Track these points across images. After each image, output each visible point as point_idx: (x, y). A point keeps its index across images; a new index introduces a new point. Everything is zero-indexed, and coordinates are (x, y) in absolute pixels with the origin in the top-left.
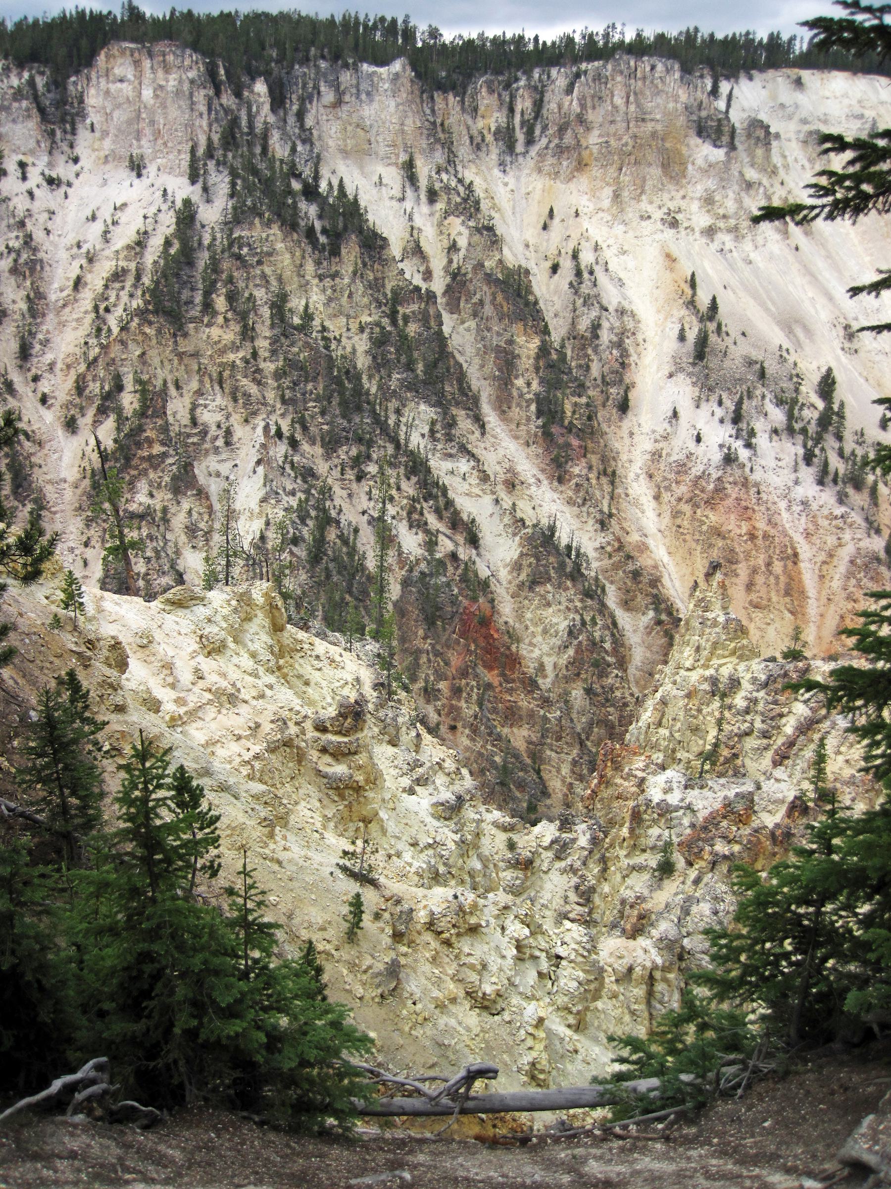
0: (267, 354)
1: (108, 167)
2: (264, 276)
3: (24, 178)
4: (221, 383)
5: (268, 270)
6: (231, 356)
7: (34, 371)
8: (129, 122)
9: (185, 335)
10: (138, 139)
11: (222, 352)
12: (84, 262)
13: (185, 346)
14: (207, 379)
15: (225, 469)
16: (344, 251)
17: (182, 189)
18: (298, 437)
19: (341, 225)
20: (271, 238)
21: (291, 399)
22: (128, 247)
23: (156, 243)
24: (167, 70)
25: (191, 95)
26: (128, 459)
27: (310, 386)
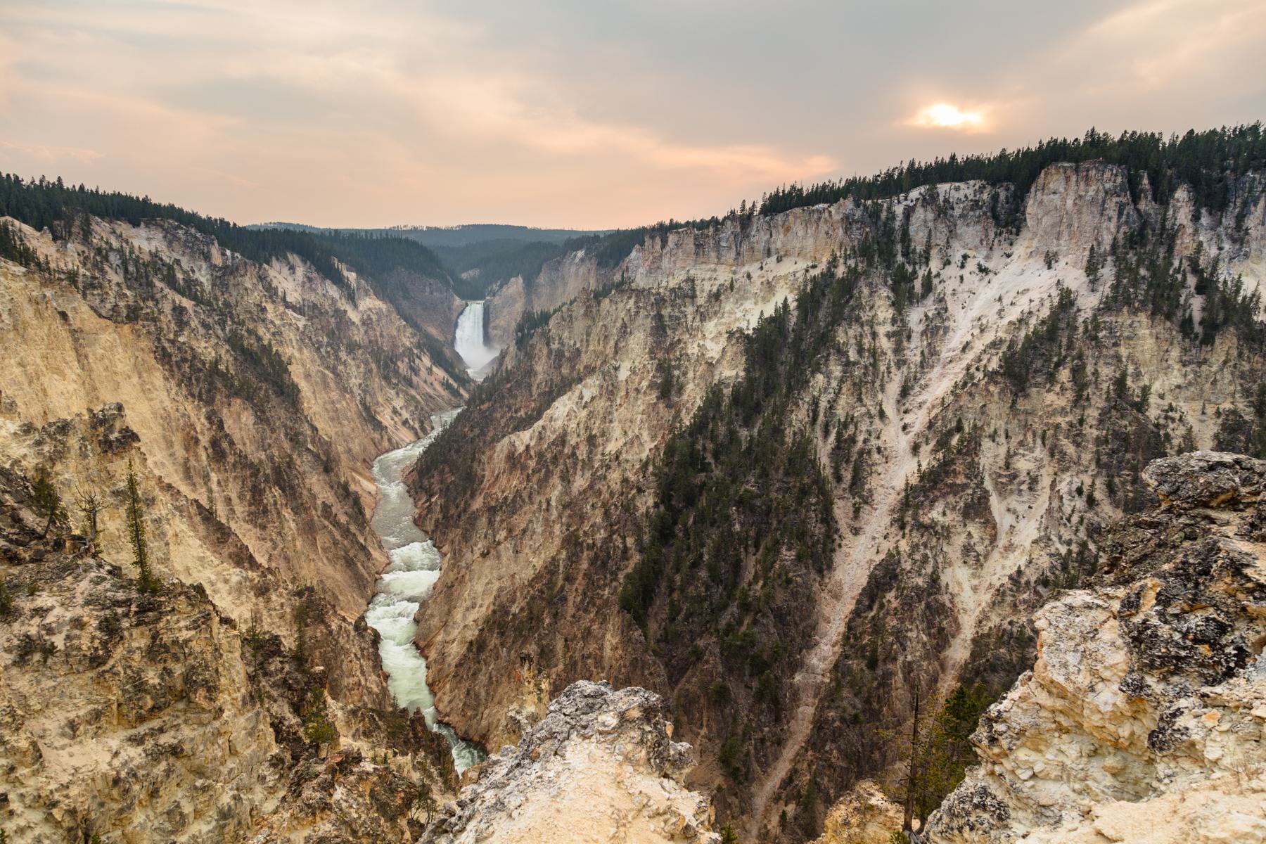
0: (1094, 422)
1: (1031, 261)
2: (1118, 358)
3: (963, 266)
4: (1043, 438)
5: (1123, 351)
6: (1059, 419)
7: (907, 405)
8: (1053, 226)
9: (1027, 396)
10: (1058, 239)
11: (1052, 414)
12: (977, 332)
13: (1022, 404)
14: (1029, 435)
15: (1021, 509)
16: (1218, 341)
17: (1075, 278)
18: (1098, 495)
19: (1221, 316)
20: (1136, 324)
21: (1105, 464)
22: (1011, 323)
23: (1033, 321)
24: (1087, 180)
25: (1104, 202)
26: (936, 483)
27: (1128, 456)
